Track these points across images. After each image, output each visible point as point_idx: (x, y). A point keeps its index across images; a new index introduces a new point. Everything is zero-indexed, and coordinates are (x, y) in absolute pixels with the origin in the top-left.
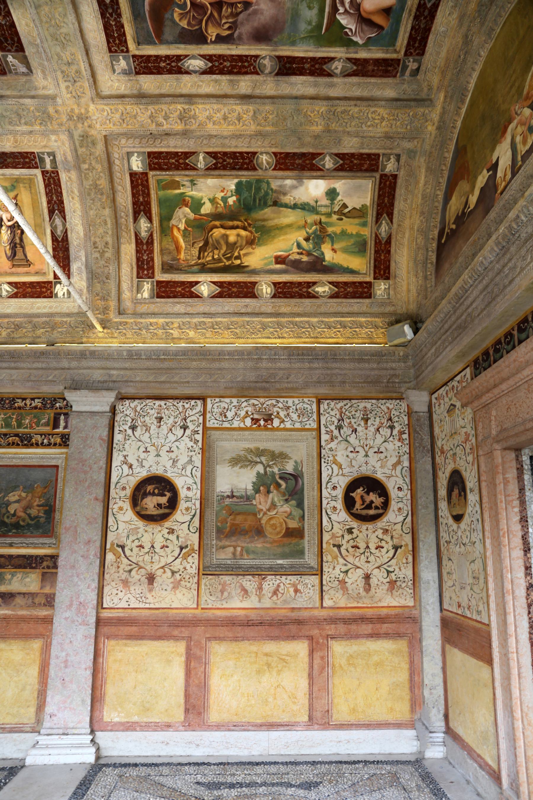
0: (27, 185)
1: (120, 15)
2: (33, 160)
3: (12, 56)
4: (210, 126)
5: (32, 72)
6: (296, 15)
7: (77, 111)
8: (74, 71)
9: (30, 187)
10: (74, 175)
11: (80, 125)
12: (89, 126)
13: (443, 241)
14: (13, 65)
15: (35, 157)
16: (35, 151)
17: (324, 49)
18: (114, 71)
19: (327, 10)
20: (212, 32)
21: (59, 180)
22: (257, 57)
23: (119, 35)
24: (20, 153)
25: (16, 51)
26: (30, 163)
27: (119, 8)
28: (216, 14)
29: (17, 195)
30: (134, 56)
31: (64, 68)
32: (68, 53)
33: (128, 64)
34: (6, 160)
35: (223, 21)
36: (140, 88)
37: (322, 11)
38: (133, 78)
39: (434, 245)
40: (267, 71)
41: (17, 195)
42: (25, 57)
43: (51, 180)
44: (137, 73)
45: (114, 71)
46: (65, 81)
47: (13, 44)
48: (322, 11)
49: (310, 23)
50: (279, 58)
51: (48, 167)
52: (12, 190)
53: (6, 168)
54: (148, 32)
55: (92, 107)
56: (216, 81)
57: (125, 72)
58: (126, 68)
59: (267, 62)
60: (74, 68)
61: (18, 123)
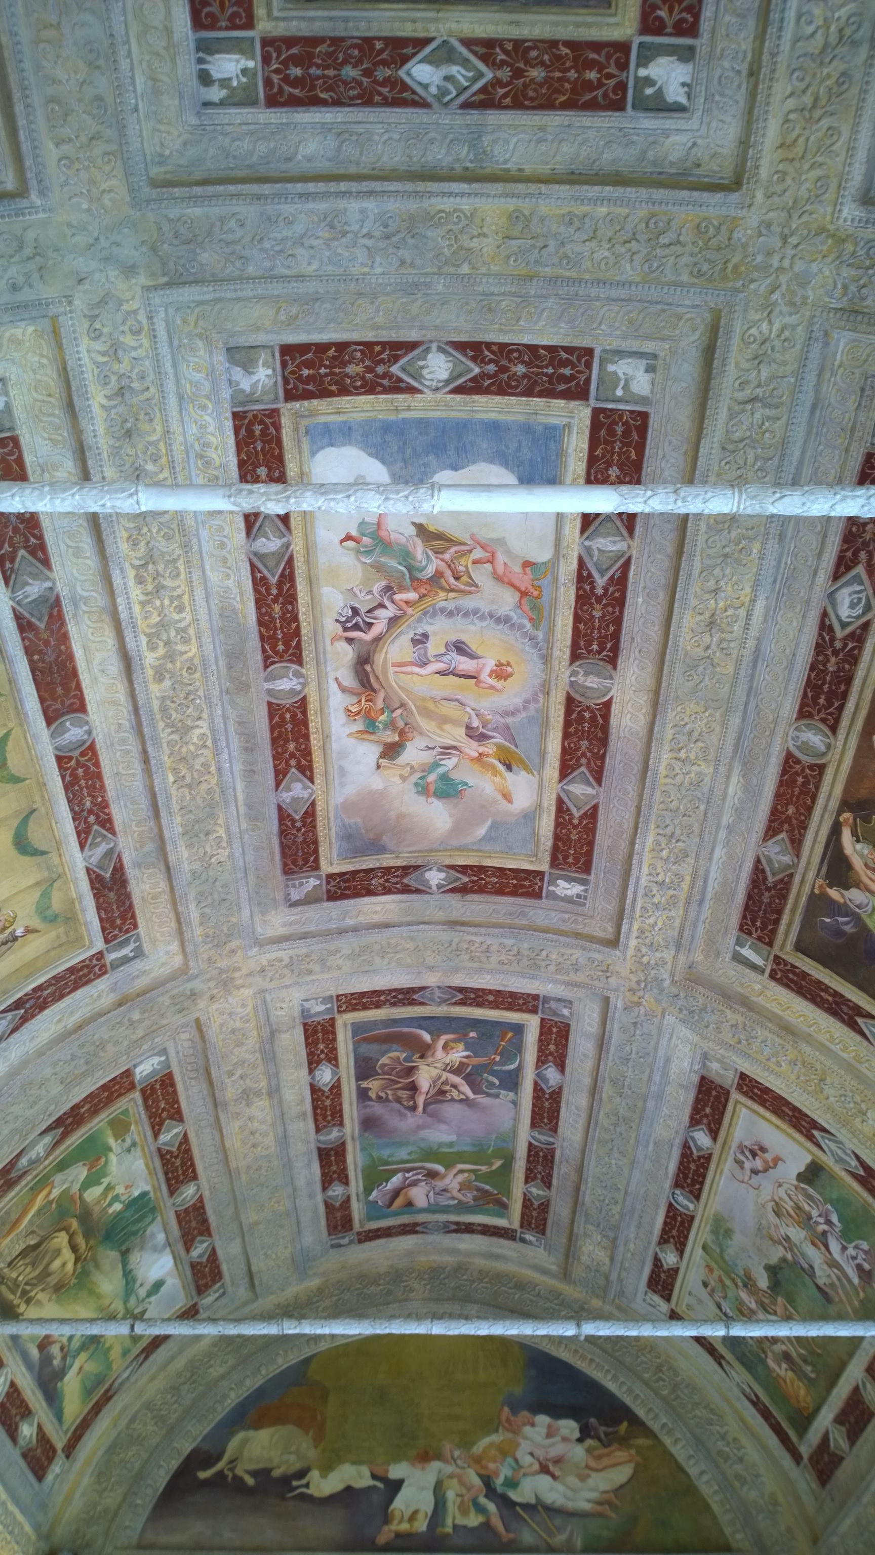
0: (64, 939)
1: (394, 1004)
2: (120, 930)
3: (320, 885)
4: (237, 1124)
5: (291, 906)
6: (400, 1144)
7: (237, 975)
8: (310, 966)
9: (60, 945)
10: (108, 1000)
11: (212, 984)
12: (212, 997)
13: (203, 1475)
14: (301, 884)
15: (127, 931)
16: (141, 930)
17: (360, 1176)
18: (307, 1000)
19: (408, 1165)
20: (374, 1085)
21: (89, 981)
22: (341, 1124)
23: (364, 1004)
24: (131, 906)
25: (328, 891)
26: (113, 926)
27: (404, 1004)
28: (399, 1086)
29: (37, 931)
30: (332, 1021)
31: (314, 957)
32: (340, 962)
33: (319, 1013)
34: (110, 890)
35: (389, 1092)
36: (280, 1032)
37: (407, 1162)
38: (298, 1021)
39: (173, 1462)
40: (322, 1138)
41: (37, 931)
42: (317, 900)
43: (86, 971)
44: (305, 1025)
45: (307, 1000)
46: (291, 958)
47: (339, 888)
48: (407, 1162)
49: (389, 1156)
50: (343, 1144)
51: (111, 957)
52: (45, 919)
53: (95, 895)
54: (371, 1030)
55: (247, 992)
56: (302, 1101)
57: (304, 1013)
58: (312, 1012)
59: (334, 1134)
60: (316, 968)
61: (203, 905)
